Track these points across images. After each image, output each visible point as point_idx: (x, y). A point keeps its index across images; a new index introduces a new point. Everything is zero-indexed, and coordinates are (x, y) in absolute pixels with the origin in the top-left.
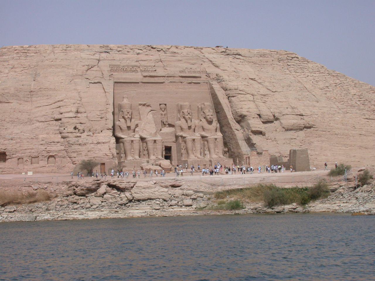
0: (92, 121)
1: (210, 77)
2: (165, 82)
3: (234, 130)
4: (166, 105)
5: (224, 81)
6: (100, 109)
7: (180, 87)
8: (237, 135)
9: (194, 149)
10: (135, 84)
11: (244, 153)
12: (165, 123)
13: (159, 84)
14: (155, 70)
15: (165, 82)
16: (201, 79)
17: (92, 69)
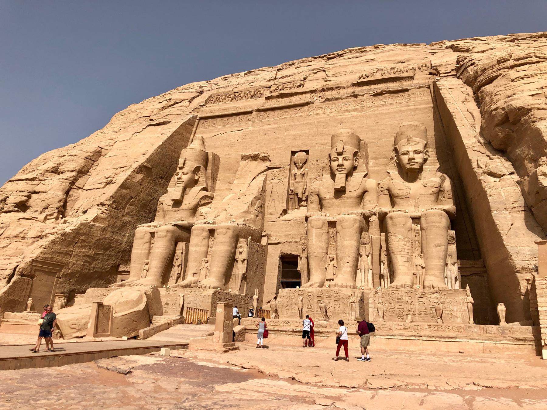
0: (87, 190)
1: (438, 73)
2: (313, 103)
3: (481, 178)
4: (307, 152)
5: (472, 64)
6: (120, 165)
7: (351, 107)
8: (489, 192)
9: (332, 254)
10: (242, 117)
11: (518, 264)
12: (300, 196)
13: (298, 109)
14: (299, 84)
15: (313, 103)
16: (415, 81)
17: (177, 105)
